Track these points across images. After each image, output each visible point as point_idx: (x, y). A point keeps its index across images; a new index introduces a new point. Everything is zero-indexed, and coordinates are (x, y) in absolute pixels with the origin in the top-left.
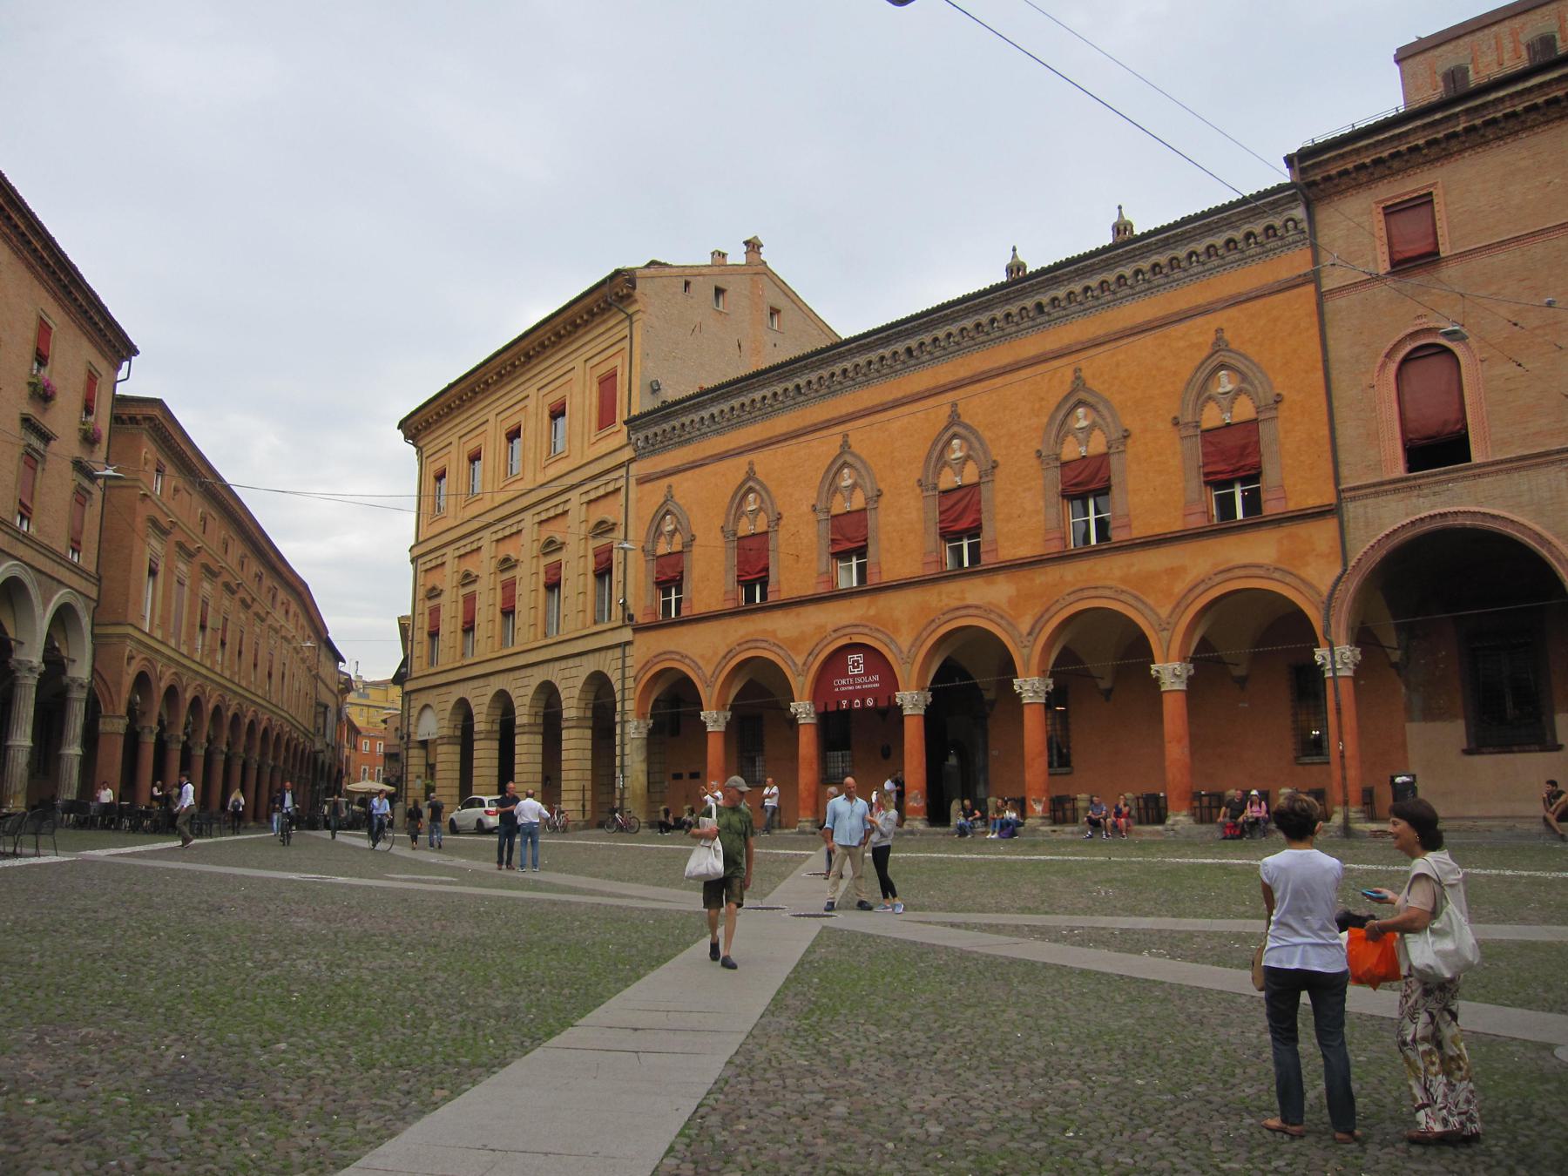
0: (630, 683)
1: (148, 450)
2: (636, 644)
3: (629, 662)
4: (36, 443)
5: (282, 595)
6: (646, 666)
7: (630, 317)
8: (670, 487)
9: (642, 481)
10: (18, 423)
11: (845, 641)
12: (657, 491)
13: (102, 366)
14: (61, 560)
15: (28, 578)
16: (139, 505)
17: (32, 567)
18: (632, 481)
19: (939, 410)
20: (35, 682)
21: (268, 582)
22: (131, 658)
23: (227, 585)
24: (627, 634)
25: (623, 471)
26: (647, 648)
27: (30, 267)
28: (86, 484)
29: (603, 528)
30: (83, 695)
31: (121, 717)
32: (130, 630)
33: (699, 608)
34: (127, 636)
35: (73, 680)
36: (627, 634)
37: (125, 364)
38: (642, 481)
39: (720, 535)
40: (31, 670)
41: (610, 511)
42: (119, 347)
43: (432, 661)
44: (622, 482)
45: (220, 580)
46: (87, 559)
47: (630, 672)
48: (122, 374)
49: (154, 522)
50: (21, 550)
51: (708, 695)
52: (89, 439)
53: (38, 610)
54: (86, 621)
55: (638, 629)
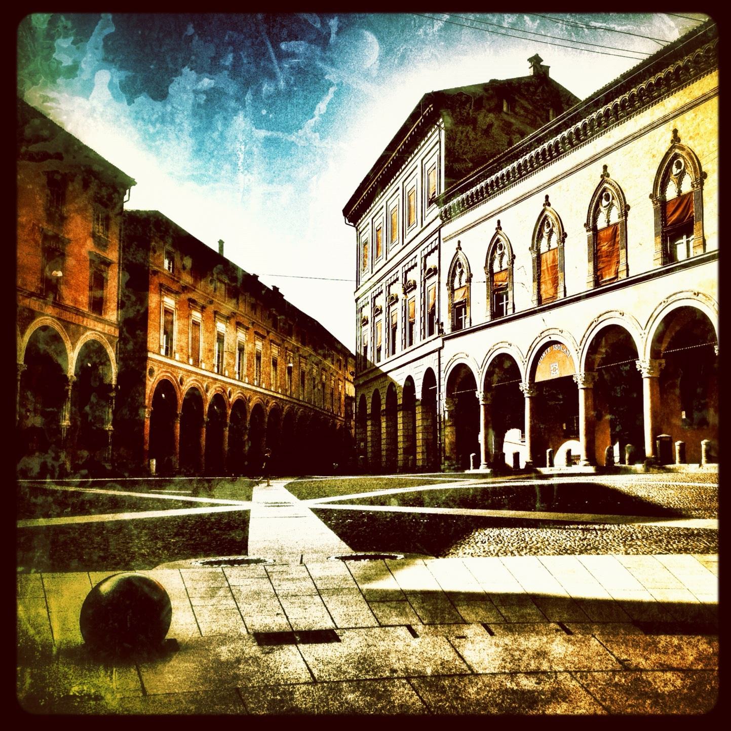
0: (443, 375)
11: (547, 340)
18: (442, 241)
19: (595, 170)
25: (437, 235)
36: (438, 343)
37: (128, 191)
41: (432, 262)
44: (437, 241)
47: (443, 368)
48: (126, 198)
51: (480, 380)
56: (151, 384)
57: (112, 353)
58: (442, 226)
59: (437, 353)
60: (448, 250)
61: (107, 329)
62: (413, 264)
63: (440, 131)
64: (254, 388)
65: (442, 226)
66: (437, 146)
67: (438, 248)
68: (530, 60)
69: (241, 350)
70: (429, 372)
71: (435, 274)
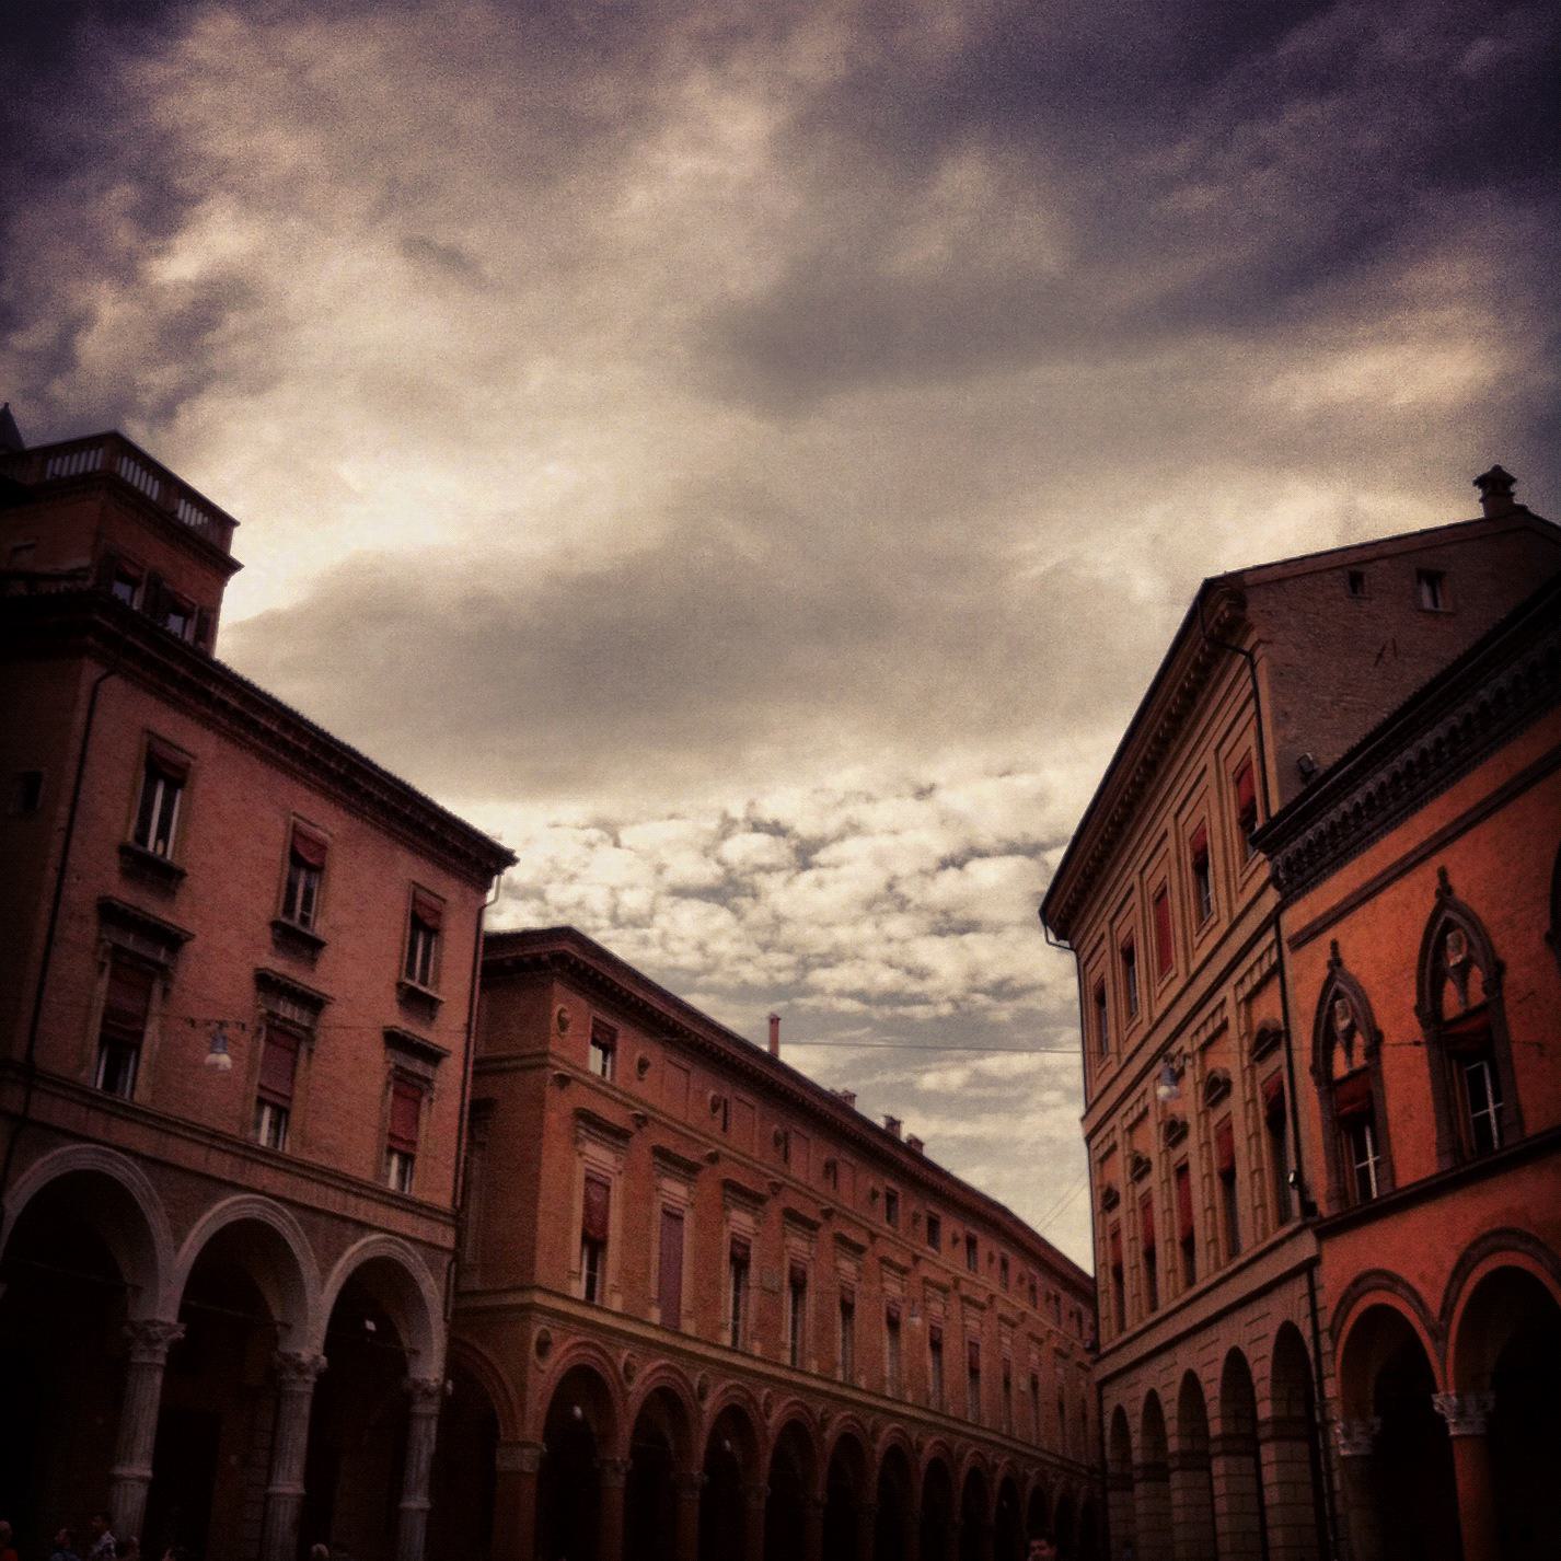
0: (1326, 1345)
1: (569, 1006)
2: (1326, 1260)
3: (1321, 1298)
4: (287, 1010)
5: (950, 1227)
6: (1347, 1301)
7: (1250, 655)
8: (1334, 945)
9: (1302, 939)
10: (247, 985)
12: (1319, 951)
13: (449, 889)
14: (372, 1192)
15: (284, 1223)
16: (550, 1092)
17: (291, 1204)
18: (1285, 947)
20: (309, 1388)
21: (910, 1205)
22: (544, 1347)
23: (791, 1216)
24: (1306, 1247)
26: (1345, 1259)
27: (264, 757)
28: (418, 1066)
29: (1268, 1041)
30: (432, 1408)
31: (526, 1445)
32: (539, 1298)
33: (1406, 1177)
34: (530, 1307)
35: (417, 1384)
36: (1306, 1247)
38: (1302, 939)
39: (1415, 1019)
40: (300, 1369)
41: (1268, 1009)
42: (482, 860)
43: (1122, 1328)
44: (1275, 950)
45: (774, 1208)
46: (436, 1182)
47: (1325, 1320)
49: (586, 1118)
50: (264, 1177)
51: (1442, 1360)
52: (418, 1002)
53: (309, 1270)
54: (432, 1289)
55: (1327, 1231)
56: (544, 1375)
57: (432, 1289)
58: (1280, 909)
59: (1304, 1277)
60: (1307, 973)
61: (422, 1229)
62: (1218, 1022)
63: (1253, 667)
64: (835, 1389)
65: (1280, 909)
66: (1251, 708)
67: (1278, 969)
68: (1481, 482)
69: (798, 1285)
70: (1288, 1333)
71: (1275, 1046)
